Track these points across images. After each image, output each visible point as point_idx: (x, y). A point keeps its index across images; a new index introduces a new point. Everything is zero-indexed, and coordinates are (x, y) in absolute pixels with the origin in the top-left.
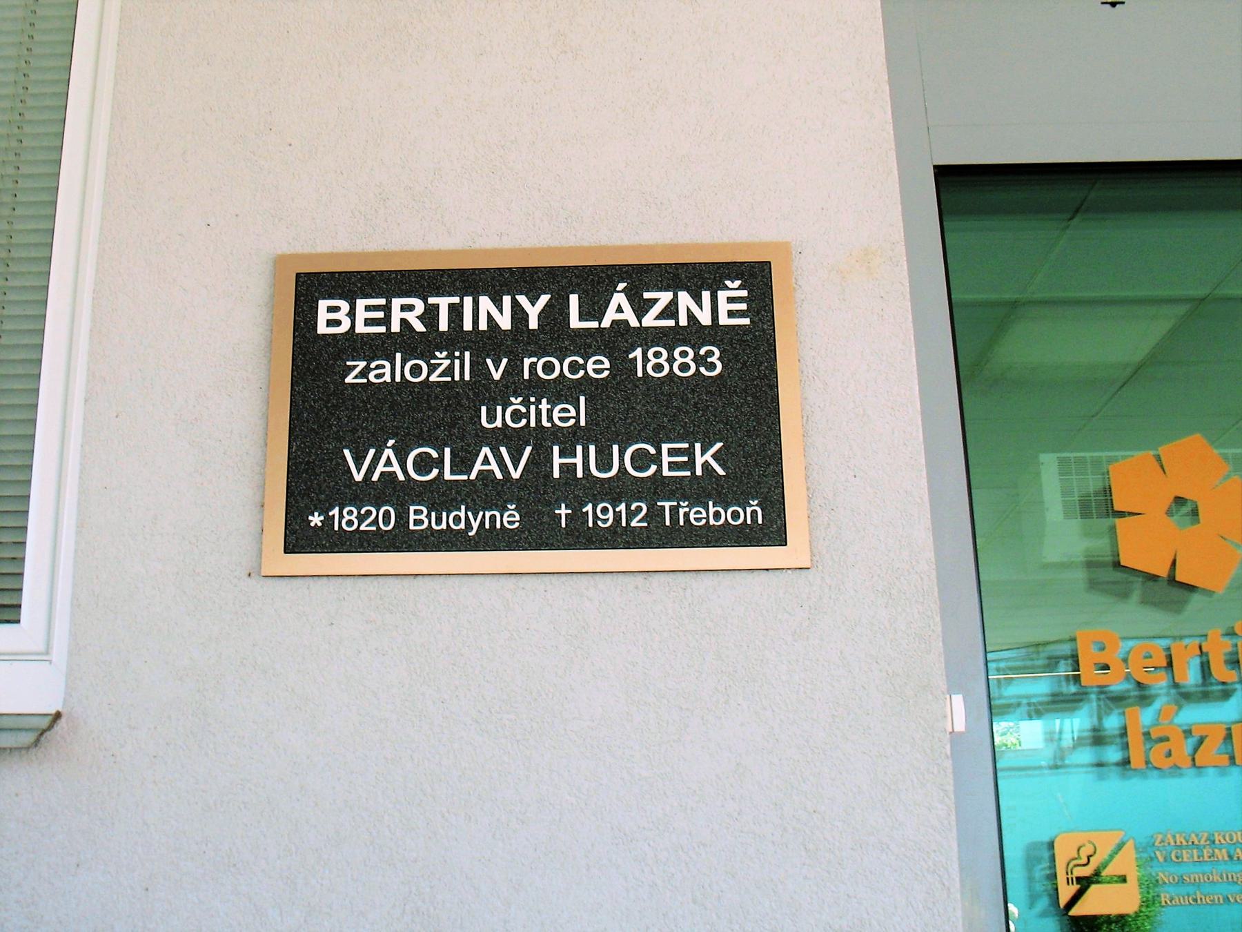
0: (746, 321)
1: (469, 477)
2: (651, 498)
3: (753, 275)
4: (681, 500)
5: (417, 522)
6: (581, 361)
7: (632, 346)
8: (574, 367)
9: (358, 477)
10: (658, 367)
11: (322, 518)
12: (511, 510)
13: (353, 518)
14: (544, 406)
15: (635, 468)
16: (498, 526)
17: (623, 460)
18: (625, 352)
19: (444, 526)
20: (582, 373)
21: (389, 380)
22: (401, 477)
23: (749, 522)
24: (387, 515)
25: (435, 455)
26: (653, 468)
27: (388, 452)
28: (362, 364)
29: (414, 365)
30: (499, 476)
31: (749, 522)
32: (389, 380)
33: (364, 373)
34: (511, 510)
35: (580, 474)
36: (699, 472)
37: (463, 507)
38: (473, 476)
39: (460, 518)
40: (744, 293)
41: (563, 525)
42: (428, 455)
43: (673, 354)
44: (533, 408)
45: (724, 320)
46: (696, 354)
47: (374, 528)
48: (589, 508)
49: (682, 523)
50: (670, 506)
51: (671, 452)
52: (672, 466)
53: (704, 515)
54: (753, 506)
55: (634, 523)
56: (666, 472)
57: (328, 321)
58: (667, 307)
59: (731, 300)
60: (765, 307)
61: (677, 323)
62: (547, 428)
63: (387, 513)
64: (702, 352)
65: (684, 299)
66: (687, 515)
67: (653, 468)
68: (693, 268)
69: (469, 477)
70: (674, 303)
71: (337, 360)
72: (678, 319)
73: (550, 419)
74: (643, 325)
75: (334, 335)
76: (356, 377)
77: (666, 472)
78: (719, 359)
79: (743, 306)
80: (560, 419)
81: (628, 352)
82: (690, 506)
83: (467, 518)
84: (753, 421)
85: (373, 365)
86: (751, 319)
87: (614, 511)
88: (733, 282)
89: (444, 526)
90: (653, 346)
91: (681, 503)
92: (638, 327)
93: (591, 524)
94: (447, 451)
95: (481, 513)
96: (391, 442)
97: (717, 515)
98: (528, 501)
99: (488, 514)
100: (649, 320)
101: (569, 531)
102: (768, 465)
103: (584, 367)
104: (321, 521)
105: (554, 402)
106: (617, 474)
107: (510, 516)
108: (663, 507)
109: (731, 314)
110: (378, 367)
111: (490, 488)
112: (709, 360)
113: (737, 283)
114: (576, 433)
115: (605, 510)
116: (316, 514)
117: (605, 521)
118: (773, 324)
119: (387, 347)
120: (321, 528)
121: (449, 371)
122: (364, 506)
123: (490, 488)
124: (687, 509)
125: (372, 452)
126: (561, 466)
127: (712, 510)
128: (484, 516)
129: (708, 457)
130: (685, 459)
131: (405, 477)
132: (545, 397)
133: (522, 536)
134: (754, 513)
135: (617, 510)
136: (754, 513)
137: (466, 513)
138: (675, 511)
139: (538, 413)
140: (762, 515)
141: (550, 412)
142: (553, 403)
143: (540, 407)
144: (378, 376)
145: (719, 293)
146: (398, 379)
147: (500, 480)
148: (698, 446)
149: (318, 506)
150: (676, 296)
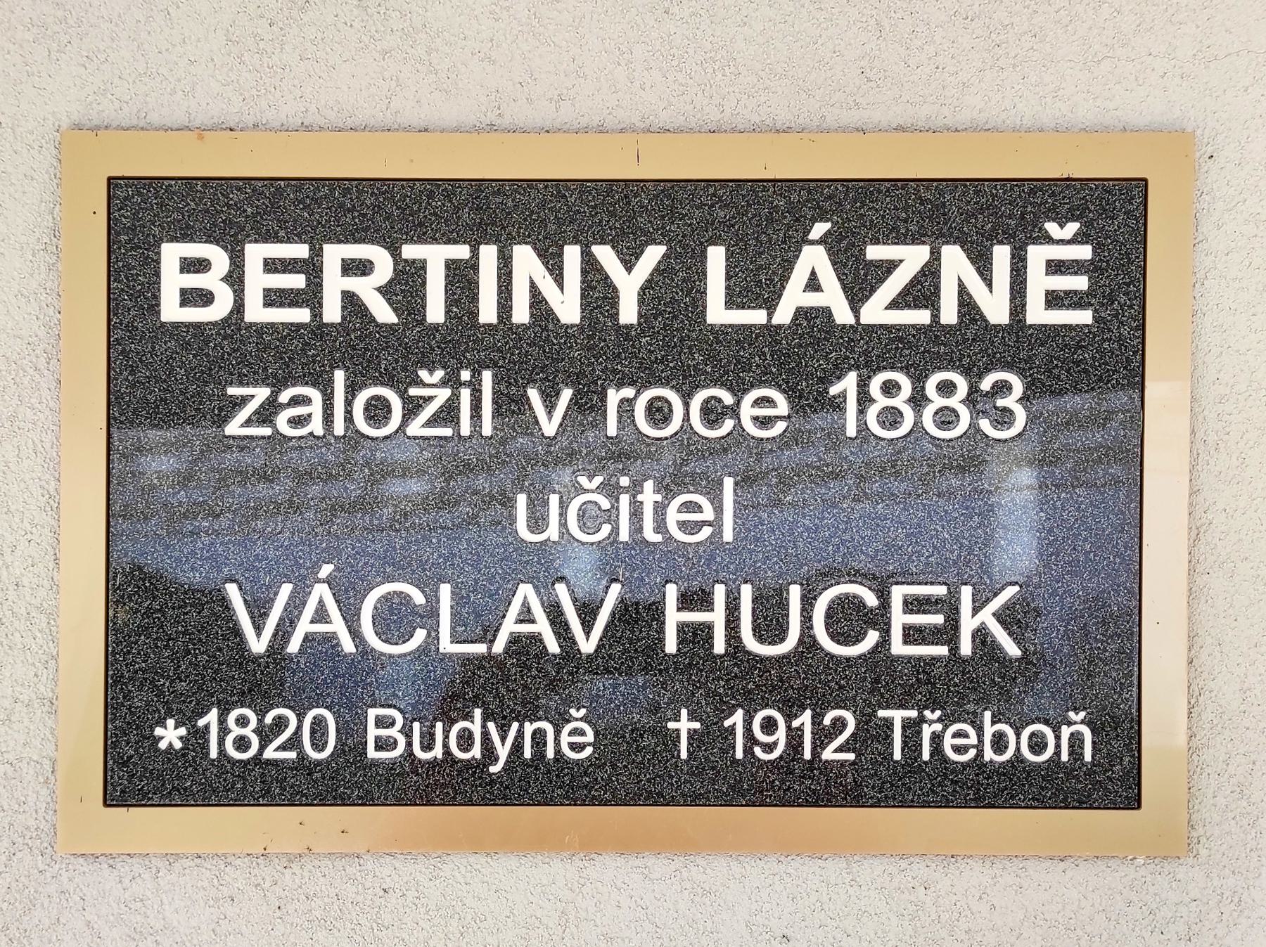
0: (1083, 317)
1: (490, 649)
2: (865, 701)
3: (1106, 212)
4: (926, 707)
5: (381, 745)
6: (728, 399)
7: (836, 366)
8: (712, 413)
9: (258, 645)
10: (891, 417)
11: (183, 731)
12: (577, 720)
13: (248, 732)
14: (649, 496)
15: (833, 637)
16: (550, 754)
17: (810, 618)
18: (821, 380)
19: (438, 752)
20: (729, 424)
21: (319, 431)
22: (348, 646)
23: (1065, 757)
24: (319, 726)
25: (418, 598)
26: (873, 637)
27: (321, 591)
28: (261, 394)
29: (372, 398)
30: (553, 647)
31: (1065, 757)
32: (319, 431)
33: (266, 414)
34: (577, 720)
35: (719, 647)
36: (966, 648)
37: (478, 713)
38: (499, 647)
39: (471, 734)
40: (1084, 252)
41: (684, 755)
42: (405, 598)
43: (923, 388)
44: (624, 499)
45: (1037, 314)
46: (973, 390)
47: (292, 755)
48: (738, 717)
49: (926, 756)
50: (903, 720)
51: (913, 605)
52: (913, 635)
53: (973, 740)
54: (1075, 723)
55: (828, 754)
56: (898, 647)
57: (183, 292)
58: (915, 281)
59: (1055, 267)
60: (1128, 285)
61: (936, 316)
62: (654, 544)
63: (319, 723)
64: (986, 384)
65: (955, 261)
66: (937, 739)
67: (873, 637)
68: (977, 192)
69: (490, 649)
70: (931, 272)
71: (206, 383)
72: (938, 310)
73: (660, 526)
74: (863, 321)
75: (197, 326)
76: (248, 423)
77: (898, 647)
78: (1020, 400)
79: (1080, 283)
80: (682, 525)
81: (826, 381)
82: (946, 721)
83: (486, 736)
84: (1086, 540)
85: (284, 397)
86: (1096, 311)
87: (789, 728)
88: (1062, 227)
89: (438, 752)
90: (880, 369)
91: (927, 713)
92: (851, 326)
93: (739, 754)
94: (445, 590)
95: (515, 725)
96: (326, 570)
97: (999, 743)
98: (611, 701)
99: (529, 728)
100: (876, 311)
101: (696, 767)
102: (1111, 637)
103: (734, 411)
104: (181, 738)
105: (667, 488)
106: (796, 648)
107: (573, 732)
108: (889, 723)
109: (1054, 300)
110: (296, 401)
111: (534, 673)
112: (1000, 403)
113: (1072, 228)
114: (712, 558)
115: (769, 725)
116: (171, 723)
117: (769, 748)
118: (1143, 327)
119: (313, 355)
120: (183, 754)
121: (448, 414)
122: (272, 707)
123: (534, 673)
124: (938, 727)
125: (286, 590)
126: (682, 628)
127: (989, 730)
128: (520, 734)
129: (987, 616)
130: (938, 619)
131: (356, 646)
132: (649, 477)
133: (600, 775)
134: (1076, 739)
135: (796, 724)
136: (1076, 739)
137: (484, 726)
138: (912, 728)
139: (636, 513)
140: (1094, 743)
141: (660, 509)
142: (667, 489)
143: (640, 498)
144: (296, 422)
145: (1032, 250)
146: (339, 428)
147: (554, 655)
148: (966, 593)
149: (174, 706)
150: (936, 255)
